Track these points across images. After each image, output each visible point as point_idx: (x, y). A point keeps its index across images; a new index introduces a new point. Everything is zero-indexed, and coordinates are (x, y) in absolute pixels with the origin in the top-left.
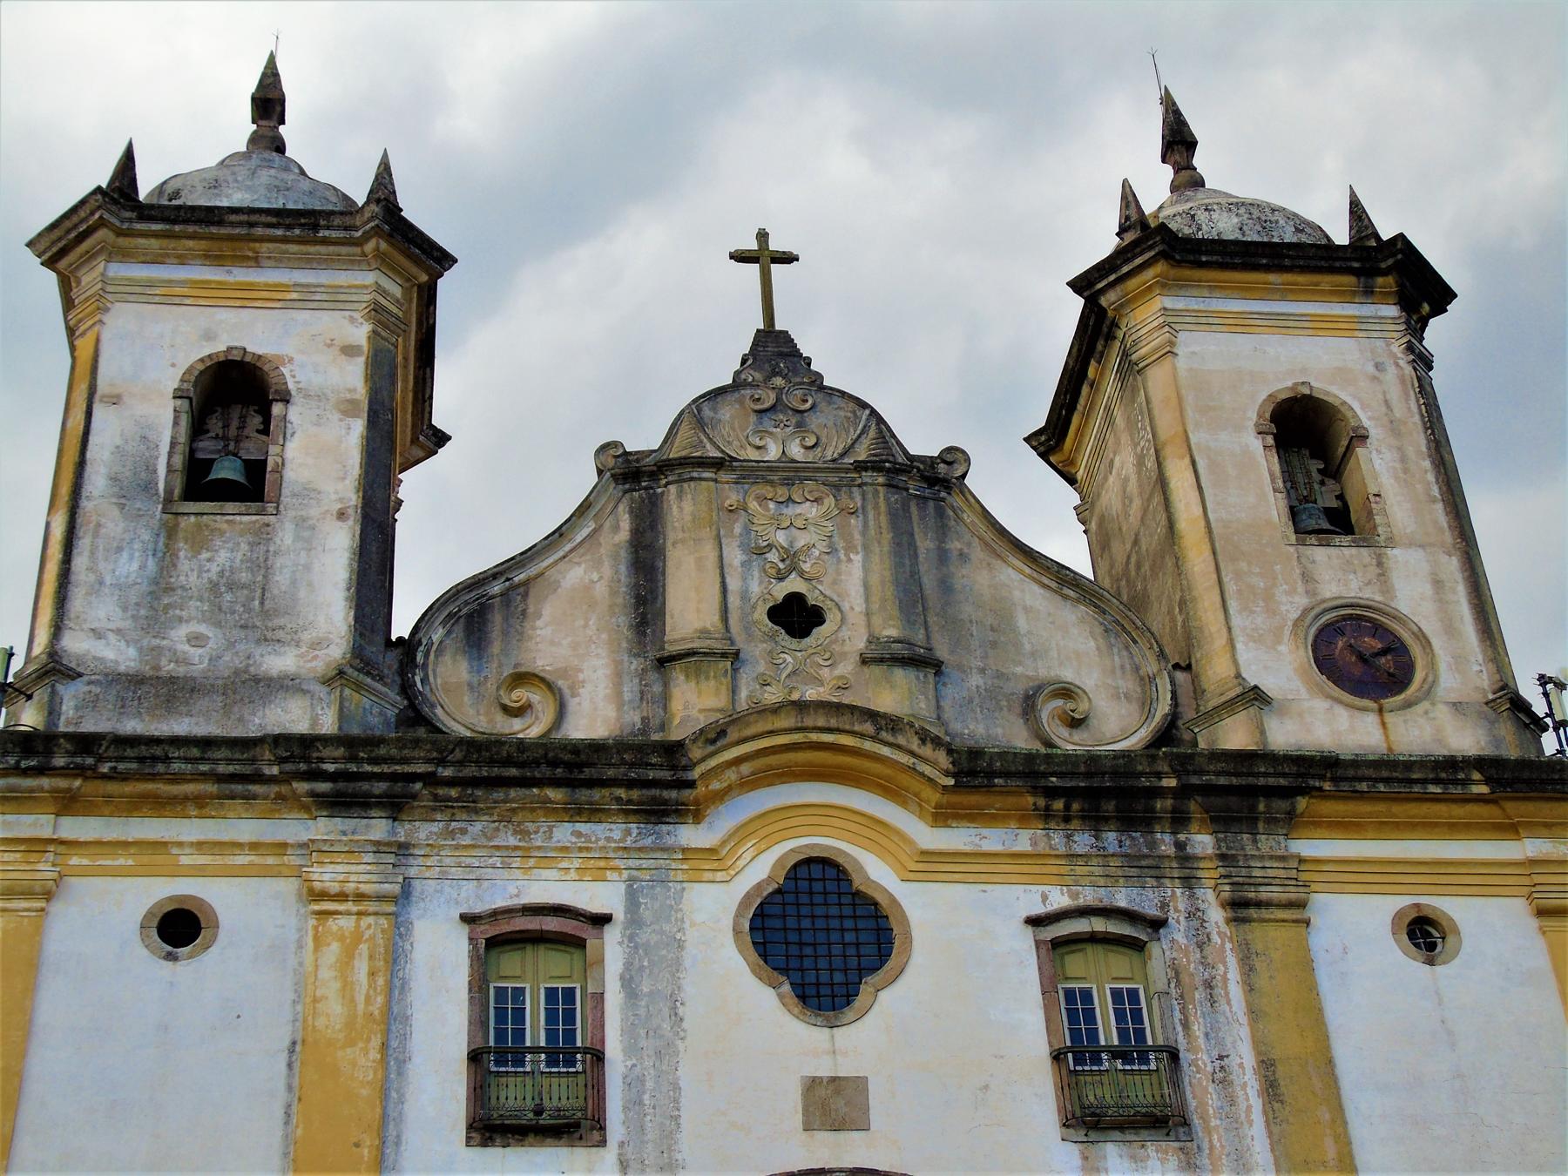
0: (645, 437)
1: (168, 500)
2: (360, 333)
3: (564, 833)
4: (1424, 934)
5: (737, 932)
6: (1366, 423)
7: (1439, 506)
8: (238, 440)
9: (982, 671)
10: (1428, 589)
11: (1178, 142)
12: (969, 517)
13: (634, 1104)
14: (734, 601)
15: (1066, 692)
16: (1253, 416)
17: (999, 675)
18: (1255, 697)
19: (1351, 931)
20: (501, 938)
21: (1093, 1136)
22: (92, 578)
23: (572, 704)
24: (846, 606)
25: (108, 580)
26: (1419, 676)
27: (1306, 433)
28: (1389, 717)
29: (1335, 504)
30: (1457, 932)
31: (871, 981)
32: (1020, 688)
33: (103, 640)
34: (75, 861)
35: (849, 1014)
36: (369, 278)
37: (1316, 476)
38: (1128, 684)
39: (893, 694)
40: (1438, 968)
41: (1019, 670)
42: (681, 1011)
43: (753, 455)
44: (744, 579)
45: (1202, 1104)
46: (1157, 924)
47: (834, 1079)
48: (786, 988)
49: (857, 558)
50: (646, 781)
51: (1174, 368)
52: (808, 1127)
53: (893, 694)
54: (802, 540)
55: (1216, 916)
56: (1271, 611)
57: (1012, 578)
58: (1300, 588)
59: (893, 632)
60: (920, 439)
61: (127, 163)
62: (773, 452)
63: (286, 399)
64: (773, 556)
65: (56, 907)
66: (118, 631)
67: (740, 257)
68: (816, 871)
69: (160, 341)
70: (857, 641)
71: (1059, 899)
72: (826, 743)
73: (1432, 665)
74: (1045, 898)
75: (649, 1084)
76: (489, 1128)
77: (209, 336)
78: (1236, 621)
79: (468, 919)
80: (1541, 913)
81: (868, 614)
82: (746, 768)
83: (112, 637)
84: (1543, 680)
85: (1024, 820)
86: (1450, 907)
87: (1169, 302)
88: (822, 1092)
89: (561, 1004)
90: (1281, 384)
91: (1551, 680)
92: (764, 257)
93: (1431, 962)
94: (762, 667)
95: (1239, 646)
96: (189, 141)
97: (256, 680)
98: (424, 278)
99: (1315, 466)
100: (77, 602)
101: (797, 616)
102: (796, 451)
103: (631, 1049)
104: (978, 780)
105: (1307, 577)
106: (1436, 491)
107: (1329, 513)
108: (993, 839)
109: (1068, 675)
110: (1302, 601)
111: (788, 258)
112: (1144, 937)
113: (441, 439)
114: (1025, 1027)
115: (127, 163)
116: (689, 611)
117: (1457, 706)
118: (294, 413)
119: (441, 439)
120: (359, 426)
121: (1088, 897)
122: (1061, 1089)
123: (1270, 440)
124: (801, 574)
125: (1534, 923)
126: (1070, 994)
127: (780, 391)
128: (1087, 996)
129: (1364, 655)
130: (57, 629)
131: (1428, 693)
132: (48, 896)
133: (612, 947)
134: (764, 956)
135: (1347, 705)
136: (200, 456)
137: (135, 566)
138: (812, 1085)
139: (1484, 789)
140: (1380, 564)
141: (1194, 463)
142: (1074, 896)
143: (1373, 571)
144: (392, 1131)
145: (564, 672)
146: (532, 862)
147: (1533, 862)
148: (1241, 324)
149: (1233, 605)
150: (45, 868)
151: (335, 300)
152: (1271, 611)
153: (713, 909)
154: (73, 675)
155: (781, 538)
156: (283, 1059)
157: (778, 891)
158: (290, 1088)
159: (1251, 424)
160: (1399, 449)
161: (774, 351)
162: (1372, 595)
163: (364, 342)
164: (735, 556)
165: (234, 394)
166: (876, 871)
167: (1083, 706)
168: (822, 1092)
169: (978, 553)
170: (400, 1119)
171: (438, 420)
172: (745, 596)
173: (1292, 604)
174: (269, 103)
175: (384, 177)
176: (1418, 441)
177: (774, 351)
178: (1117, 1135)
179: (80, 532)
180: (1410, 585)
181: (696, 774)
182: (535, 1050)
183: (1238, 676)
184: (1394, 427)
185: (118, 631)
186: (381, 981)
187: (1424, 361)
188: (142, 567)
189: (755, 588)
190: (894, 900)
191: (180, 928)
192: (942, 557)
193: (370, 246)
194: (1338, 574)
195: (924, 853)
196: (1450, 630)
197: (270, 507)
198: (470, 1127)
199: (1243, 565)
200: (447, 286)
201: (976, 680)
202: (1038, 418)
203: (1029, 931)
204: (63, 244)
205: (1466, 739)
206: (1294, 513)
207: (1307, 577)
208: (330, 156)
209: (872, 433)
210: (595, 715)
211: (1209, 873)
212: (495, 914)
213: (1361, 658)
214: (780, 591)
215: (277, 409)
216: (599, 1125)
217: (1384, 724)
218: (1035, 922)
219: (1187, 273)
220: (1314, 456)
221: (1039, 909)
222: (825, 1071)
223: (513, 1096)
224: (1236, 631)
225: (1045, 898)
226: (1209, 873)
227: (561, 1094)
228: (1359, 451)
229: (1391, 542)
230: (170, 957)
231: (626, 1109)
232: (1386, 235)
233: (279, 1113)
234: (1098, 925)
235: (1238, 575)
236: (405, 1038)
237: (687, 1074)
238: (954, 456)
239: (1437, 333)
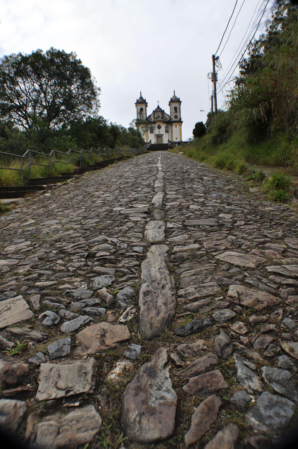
0: (154, 110)
4: (176, 126)
19: (174, 126)
27: (176, 108)
39: (161, 119)
50: (154, 123)
53: (161, 119)
69: (139, 107)
72: (159, 121)
101: (159, 117)
114: (164, 130)
116: (156, 117)
129: (176, 117)
153: (156, 126)
161: (158, 106)
177: (158, 106)
180: (178, 114)
194: (176, 114)
204: (136, 104)
210: (153, 120)
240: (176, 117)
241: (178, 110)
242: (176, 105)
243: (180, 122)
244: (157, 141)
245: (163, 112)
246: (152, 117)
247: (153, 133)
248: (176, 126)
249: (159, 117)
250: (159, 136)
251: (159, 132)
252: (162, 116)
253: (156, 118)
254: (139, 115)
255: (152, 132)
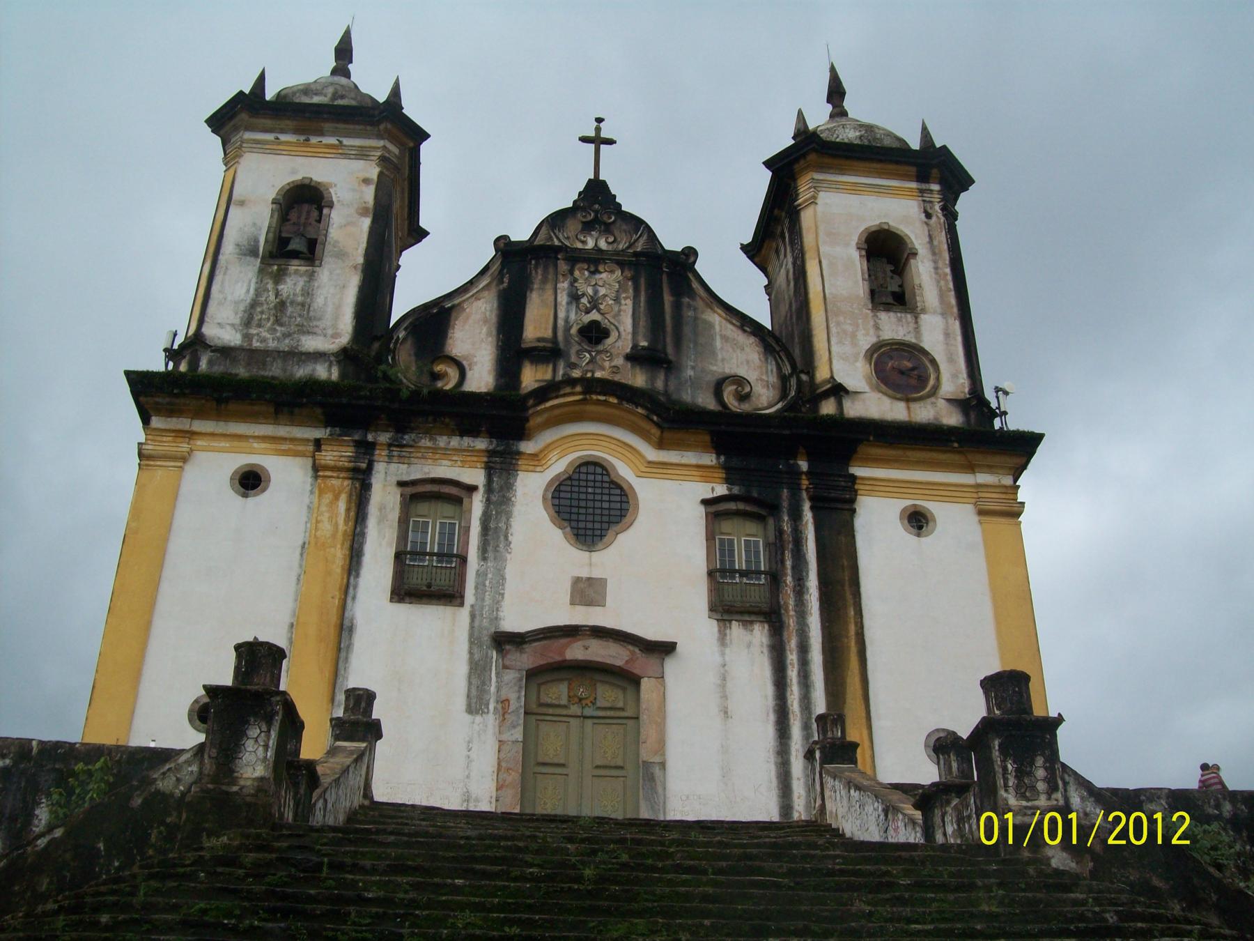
0: (521, 232)
1: (263, 258)
2: (373, 172)
3: (455, 442)
4: (918, 520)
5: (544, 498)
6: (917, 246)
7: (953, 293)
8: (305, 225)
9: (693, 368)
10: (941, 337)
11: (836, 93)
12: (695, 285)
13: (480, 587)
14: (561, 323)
15: (739, 381)
16: (855, 239)
17: (703, 371)
18: (838, 391)
20: (418, 495)
21: (725, 617)
22: (221, 296)
23: (469, 374)
24: (621, 329)
25: (229, 298)
26: (932, 382)
27: (884, 249)
28: (914, 406)
29: (897, 289)
30: (935, 521)
31: (614, 528)
32: (712, 379)
33: (224, 329)
34: (199, 443)
35: (600, 545)
36: (381, 143)
37: (890, 274)
38: (773, 379)
40: (923, 539)
41: (714, 368)
42: (510, 538)
43: (580, 246)
44: (568, 311)
45: (786, 604)
46: (773, 509)
47: (589, 579)
48: (568, 529)
49: (629, 302)
51: (815, 211)
52: (572, 603)
54: (602, 291)
55: (807, 506)
56: (854, 344)
57: (716, 319)
58: (872, 331)
59: (644, 344)
60: (672, 242)
61: (261, 79)
62: (590, 244)
63: (331, 206)
64: (584, 300)
65: (188, 467)
66: (233, 325)
67: (585, 140)
68: (591, 469)
70: (626, 345)
71: (721, 490)
73: (938, 379)
74: (713, 489)
75: (490, 576)
76: (403, 592)
77: (294, 172)
78: (834, 349)
79: (401, 484)
80: (981, 513)
81: (635, 333)
82: (557, 412)
83: (228, 328)
84: (997, 390)
85: (704, 449)
86: (933, 507)
87: (817, 176)
88: (582, 585)
89: (447, 533)
90: (873, 222)
91: (1001, 390)
92: (598, 141)
93: (919, 535)
94: (573, 359)
95: (834, 362)
96: (298, 68)
97: (302, 354)
98: (411, 145)
99: (889, 268)
100: (211, 309)
102: (603, 244)
103: (483, 555)
104: (672, 421)
105: (877, 327)
106: (951, 285)
107: (894, 294)
108: (690, 457)
109: (742, 372)
110: (873, 340)
111: (610, 142)
112: (763, 512)
113: (425, 234)
115: (261, 79)
116: (535, 327)
117: (949, 400)
118: (334, 214)
119: (421, 234)
120: (366, 222)
121: (736, 490)
122: (710, 591)
123: (864, 253)
124: (599, 310)
125: (976, 518)
126: (722, 542)
127: (596, 212)
128: (731, 542)
129: (902, 368)
130: (201, 321)
131: (934, 392)
132: (184, 459)
133: (477, 505)
134: (558, 512)
135: (889, 396)
136: (284, 235)
137: (244, 291)
138: (577, 581)
139: (956, 445)
140: (916, 322)
141: (820, 262)
142: (729, 489)
143: (912, 325)
144: (351, 590)
145: (466, 358)
146: (437, 456)
147: (978, 486)
148: (855, 189)
149: (834, 340)
150: (184, 447)
151: (362, 154)
152: (854, 344)
154: (207, 346)
155: (590, 291)
156: (298, 551)
157: (570, 478)
158: (301, 566)
159: (854, 243)
160: (935, 262)
161: (596, 192)
162: (911, 339)
163: (375, 177)
164: (563, 298)
165: (303, 202)
166: (624, 471)
167: (747, 389)
168: (582, 585)
169: (700, 304)
170: (355, 587)
171: (423, 223)
172: (567, 320)
173: (866, 341)
174: (344, 52)
175: (396, 92)
176: (946, 256)
177: (596, 192)
178: (738, 617)
179: (217, 272)
180: (934, 333)
181: (530, 412)
182: (432, 554)
183: (832, 377)
184: (934, 252)
185: (233, 325)
186: (352, 514)
187: (951, 216)
188: (248, 291)
189: (573, 316)
190: (631, 487)
191: (250, 481)
192: (677, 306)
193: (382, 127)
194: (893, 327)
195: (650, 462)
196: (951, 360)
197: (317, 262)
198: (393, 593)
199: (841, 319)
200: (424, 147)
201: (690, 373)
202: (748, 239)
203: (702, 509)
205: (952, 419)
206: (873, 293)
207: (877, 327)
208: (371, 81)
209: (645, 237)
210: (481, 378)
211: (805, 482)
212: (414, 483)
213: (902, 373)
214: (587, 318)
215: (325, 211)
216: (462, 597)
217: (908, 408)
218: (705, 502)
219: (827, 160)
220: (889, 262)
221: (709, 496)
222: (584, 573)
223: (416, 580)
224: (833, 353)
225: (713, 489)
226: (805, 482)
227: (442, 581)
228: (912, 261)
229: (924, 311)
230: (245, 496)
231: (476, 588)
232: (938, 145)
233: (294, 579)
234: (741, 506)
235: (838, 324)
236: (361, 545)
237: (510, 571)
238: (690, 253)
239: (964, 204)
240: (902, 368)
241: (926, 274)
242: (899, 208)
243: (989, 445)
244: (530, 765)
245: (667, 276)
246: (474, 352)
247: (450, 596)
248: (918, 520)
249: (594, 334)
250: (579, 678)
251: (587, 591)
252: (653, 316)
253: (549, 353)
254: (239, 283)
255: (426, 580)
